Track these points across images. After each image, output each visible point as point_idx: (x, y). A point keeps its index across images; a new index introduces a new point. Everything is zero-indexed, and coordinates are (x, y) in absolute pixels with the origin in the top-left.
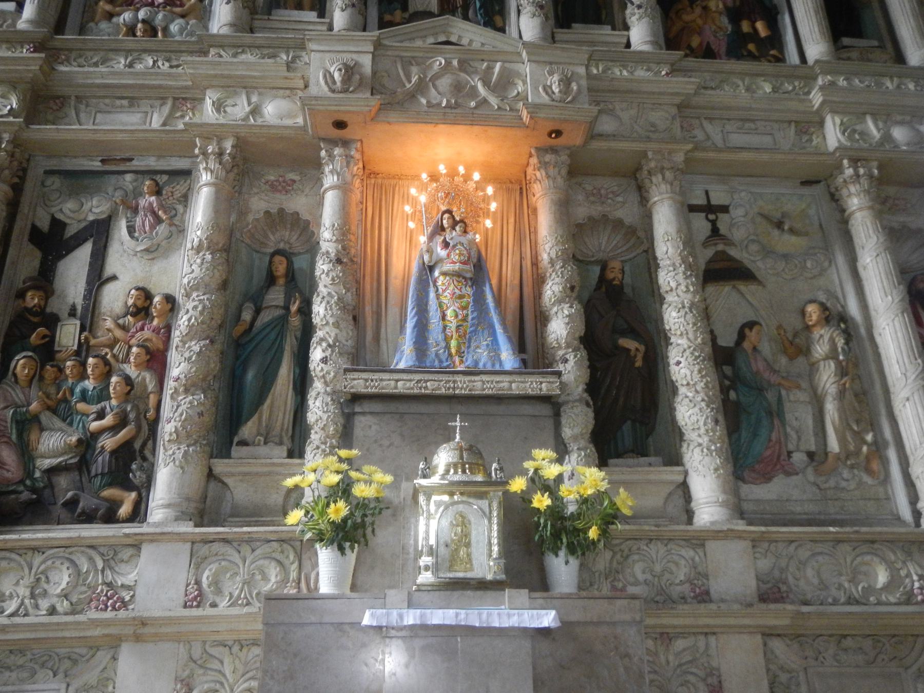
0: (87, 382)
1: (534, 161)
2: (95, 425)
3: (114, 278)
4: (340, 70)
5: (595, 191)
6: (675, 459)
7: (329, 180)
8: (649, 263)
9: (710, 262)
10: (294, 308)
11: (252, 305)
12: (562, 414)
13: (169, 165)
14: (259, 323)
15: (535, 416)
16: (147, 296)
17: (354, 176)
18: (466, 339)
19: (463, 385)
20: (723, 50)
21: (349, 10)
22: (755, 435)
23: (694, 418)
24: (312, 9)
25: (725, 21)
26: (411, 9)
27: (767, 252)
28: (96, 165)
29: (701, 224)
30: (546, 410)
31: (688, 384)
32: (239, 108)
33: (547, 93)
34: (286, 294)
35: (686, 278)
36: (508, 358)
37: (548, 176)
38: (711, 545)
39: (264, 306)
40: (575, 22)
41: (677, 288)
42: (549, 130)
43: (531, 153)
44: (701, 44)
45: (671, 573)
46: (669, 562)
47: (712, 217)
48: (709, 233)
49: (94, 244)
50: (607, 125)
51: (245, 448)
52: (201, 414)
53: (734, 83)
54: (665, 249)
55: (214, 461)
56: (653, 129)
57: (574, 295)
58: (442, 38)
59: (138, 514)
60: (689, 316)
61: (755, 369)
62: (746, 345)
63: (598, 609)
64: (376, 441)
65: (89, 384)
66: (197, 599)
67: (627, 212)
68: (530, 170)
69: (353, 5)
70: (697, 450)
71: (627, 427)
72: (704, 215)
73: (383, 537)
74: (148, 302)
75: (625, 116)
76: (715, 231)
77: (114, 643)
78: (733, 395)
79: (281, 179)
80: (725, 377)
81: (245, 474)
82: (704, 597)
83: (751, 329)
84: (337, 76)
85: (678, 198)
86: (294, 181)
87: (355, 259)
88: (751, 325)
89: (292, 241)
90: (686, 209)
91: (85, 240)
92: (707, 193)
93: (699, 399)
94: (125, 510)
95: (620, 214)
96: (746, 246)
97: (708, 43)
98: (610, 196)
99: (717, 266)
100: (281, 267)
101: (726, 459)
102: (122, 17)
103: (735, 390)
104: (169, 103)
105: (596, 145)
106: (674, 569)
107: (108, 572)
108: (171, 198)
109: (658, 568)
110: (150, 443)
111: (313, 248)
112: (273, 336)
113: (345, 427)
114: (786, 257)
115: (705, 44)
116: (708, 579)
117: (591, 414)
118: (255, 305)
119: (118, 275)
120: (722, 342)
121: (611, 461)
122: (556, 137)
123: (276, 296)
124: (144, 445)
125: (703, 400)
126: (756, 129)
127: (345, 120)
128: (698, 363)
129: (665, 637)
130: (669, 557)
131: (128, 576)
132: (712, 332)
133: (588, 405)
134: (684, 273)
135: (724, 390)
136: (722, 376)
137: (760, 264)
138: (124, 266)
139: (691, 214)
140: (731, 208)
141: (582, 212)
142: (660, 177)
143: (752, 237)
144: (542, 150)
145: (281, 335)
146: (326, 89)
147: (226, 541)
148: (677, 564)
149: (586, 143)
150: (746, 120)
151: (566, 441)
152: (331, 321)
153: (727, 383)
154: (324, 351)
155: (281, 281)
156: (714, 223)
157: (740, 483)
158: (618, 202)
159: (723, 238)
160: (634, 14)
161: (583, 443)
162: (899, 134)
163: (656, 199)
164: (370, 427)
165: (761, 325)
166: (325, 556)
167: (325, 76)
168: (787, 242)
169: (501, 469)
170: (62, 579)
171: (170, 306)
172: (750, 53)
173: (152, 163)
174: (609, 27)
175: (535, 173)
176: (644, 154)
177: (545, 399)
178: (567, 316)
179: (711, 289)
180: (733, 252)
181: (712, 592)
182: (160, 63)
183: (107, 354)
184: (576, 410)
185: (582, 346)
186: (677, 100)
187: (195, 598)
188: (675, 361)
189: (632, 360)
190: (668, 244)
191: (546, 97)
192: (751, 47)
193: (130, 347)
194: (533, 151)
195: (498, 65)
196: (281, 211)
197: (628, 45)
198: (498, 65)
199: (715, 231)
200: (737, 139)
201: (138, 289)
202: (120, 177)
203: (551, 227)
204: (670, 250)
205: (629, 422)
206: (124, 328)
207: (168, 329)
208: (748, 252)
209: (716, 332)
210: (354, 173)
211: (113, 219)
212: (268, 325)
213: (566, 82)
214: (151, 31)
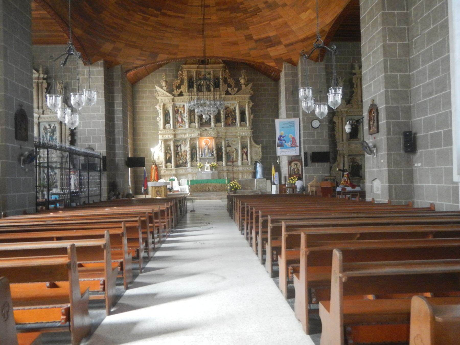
6: (222, 161)
7: (197, 141)
16: (185, 151)
18: (208, 154)
19: (208, 158)
27: (232, 144)
29: (227, 142)
32: (190, 135)
36: (211, 155)
50: (219, 134)
59: (187, 166)
63: (215, 171)
65: (182, 157)
66: (192, 171)
67: (221, 141)
73: (203, 167)
76: (228, 143)
77: (188, 174)
82: (223, 170)
111: (196, 145)
114: (234, 144)
123: (194, 150)
129: (220, 173)
131: (188, 170)
141: (217, 141)
150: (231, 133)
162: (243, 134)
166: (200, 169)
168: (234, 143)
170: (184, 170)
197: (221, 126)
199: (228, 143)
200: (230, 134)
207: (187, 153)
213: (215, 133)
214: (181, 126)
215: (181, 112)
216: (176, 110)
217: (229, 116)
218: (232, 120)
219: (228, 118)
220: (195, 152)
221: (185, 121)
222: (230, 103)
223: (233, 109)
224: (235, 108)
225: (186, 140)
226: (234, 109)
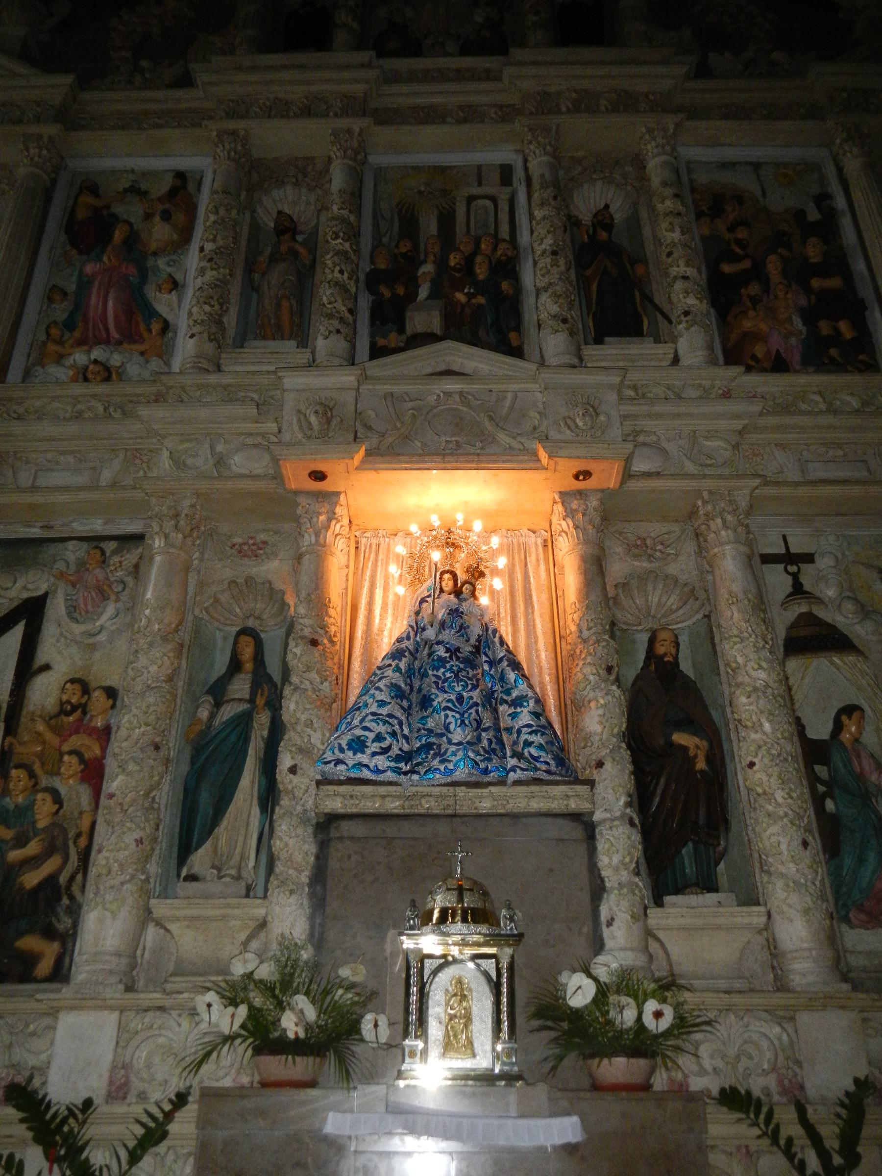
0: (8, 799)
1: (559, 508)
2: (15, 855)
3: (47, 667)
4: (316, 412)
5: (639, 543)
8: (712, 632)
9: (792, 627)
10: (260, 701)
11: (210, 698)
12: (598, 837)
13: (118, 529)
14: (217, 722)
15: (562, 840)
17: (336, 535)
20: (797, 358)
21: (334, 337)
22: (861, 861)
23: (774, 839)
24: (289, 339)
25: (798, 323)
26: (409, 331)
28: (35, 532)
30: (576, 832)
31: (765, 793)
33: (569, 428)
34: (252, 683)
35: (758, 650)
37: (576, 527)
38: (804, 1018)
39: (225, 698)
40: (609, 336)
41: (746, 665)
42: (574, 471)
43: (554, 498)
44: (768, 352)
45: (750, 1057)
46: (746, 1042)
47: (793, 569)
48: (789, 589)
49: (27, 626)
51: (194, 884)
52: (139, 842)
53: (812, 400)
54: (729, 614)
55: (153, 902)
56: (709, 462)
57: (612, 677)
58: (442, 367)
60: (762, 702)
61: (858, 770)
62: (846, 737)
64: (356, 876)
68: (555, 520)
69: (338, 331)
70: (780, 884)
71: (687, 851)
72: (782, 566)
74: (86, 697)
75: (671, 447)
76: (798, 590)
78: (830, 805)
79: (251, 542)
80: (818, 780)
81: (192, 919)
83: (850, 717)
84: (313, 419)
85: (744, 549)
86: (265, 543)
87: (335, 639)
88: (850, 710)
89: (265, 617)
90: (757, 560)
91: (16, 623)
92: (784, 538)
93: (781, 813)
94: (44, 967)
95: (672, 569)
96: (840, 605)
97: (778, 351)
98: (659, 547)
99: (803, 632)
100: (247, 652)
101: (823, 897)
102: (72, 357)
103: (832, 798)
104: (122, 455)
105: (634, 485)
106: (754, 1052)
107: (16, 1050)
108: (119, 569)
109: (732, 1052)
110: (79, 877)
112: (233, 738)
113: (317, 857)
115: (774, 353)
116: (801, 1067)
117: (637, 837)
118: (215, 699)
119: (52, 664)
120: (811, 734)
121: (668, 899)
122: (585, 479)
123: (240, 687)
124: (72, 879)
125: (786, 815)
126: (845, 455)
127: (323, 469)
128: (777, 765)
130: (745, 1035)
132: (798, 720)
133: (632, 823)
134: (755, 646)
135: (818, 801)
136: (813, 780)
137: (858, 628)
138: (60, 653)
139: (765, 567)
140: (816, 556)
142: (719, 521)
143: (848, 593)
144: (565, 496)
145: (245, 740)
146: (300, 436)
147: (161, 1009)
148: (756, 1045)
149: (623, 482)
151: (604, 873)
152: (303, 718)
153: (821, 788)
154: (292, 758)
155: (249, 666)
156: (795, 576)
157: (844, 927)
158: (669, 554)
159: (809, 596)
160: (680, 323)
161: (625, 875)
163: (716, 550)
164: (349, 856)
165: (862, 710)
167: (299, 420)
169: (511, 919)
171: (110, 702)
172: (832, 360)
173: (97, 526)
174: (652, 339)
175: (561, 524)
176: (698, 493)
177: (576, 817)
178: (605, 706)
179: (793, 664)
180: (821, 613)
181: (808, 1085)
182: (111, 410)
183: (34, 763)
184: (615, 832)
185: (624, 745)
186: (738, 424)
187: (120, 1088)
188: (745, 763)
189: (692, 760)
190: (734, 608)
191: (568, 432)
192: (833, 352)
193: (61, 755)
194: (557, 497)
195: (510, 396)
196: (250, 581)
197: (676, 361)
198: (510, 396)
199: (798, 590)
201: (73, 681)
202: (60, 545)
203: (580, 591)
204: (736, 615)
205: (690, 845)
206: (56, 730)
208: (842, 614)
209: (804, 721)
210: (337, 532)
211: (50, 596)
212: (227, 724)
215: (132, 241)
216: (81, 215)
217: (757, 273)
218: (810, 317)
219: (754, 289)
220: (244, 722)
221: (166, 326)
222: (757, 166)
223: (800, 214)
224: (823, 199)
225: (138, 538)
226: (814, 215)
